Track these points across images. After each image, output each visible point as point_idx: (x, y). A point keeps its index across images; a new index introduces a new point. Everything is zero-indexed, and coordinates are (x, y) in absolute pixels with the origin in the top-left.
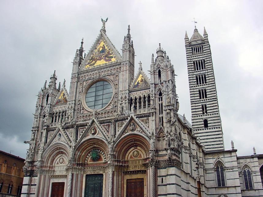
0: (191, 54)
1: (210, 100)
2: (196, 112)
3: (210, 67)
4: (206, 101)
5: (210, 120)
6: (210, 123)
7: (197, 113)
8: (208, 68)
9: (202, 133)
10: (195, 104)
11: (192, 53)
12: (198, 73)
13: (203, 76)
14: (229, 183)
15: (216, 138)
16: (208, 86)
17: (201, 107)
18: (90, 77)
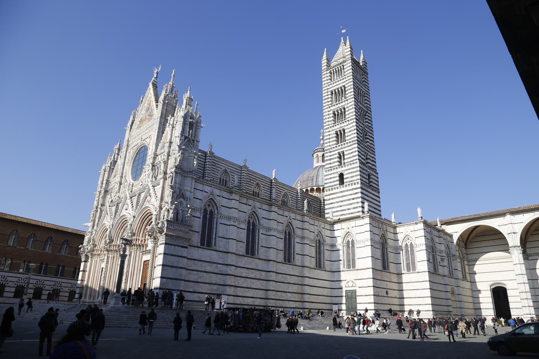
0: (329, 81)
1: (349, 144)
2: (330, 164)
3: (351, 95)
4: (343, 146)
5: (347, 174)
6: (347, 178)
7: (332, 165)
8: (349, 96)
9: (336, 193)
10: (330, 152)
11: (331, 79)
12: (336, 107)
13: (343, 110)
14: (359, 264)
15: (353, 199)
16: (347, 123)
17: (337, 155)
18: (136, 143)
